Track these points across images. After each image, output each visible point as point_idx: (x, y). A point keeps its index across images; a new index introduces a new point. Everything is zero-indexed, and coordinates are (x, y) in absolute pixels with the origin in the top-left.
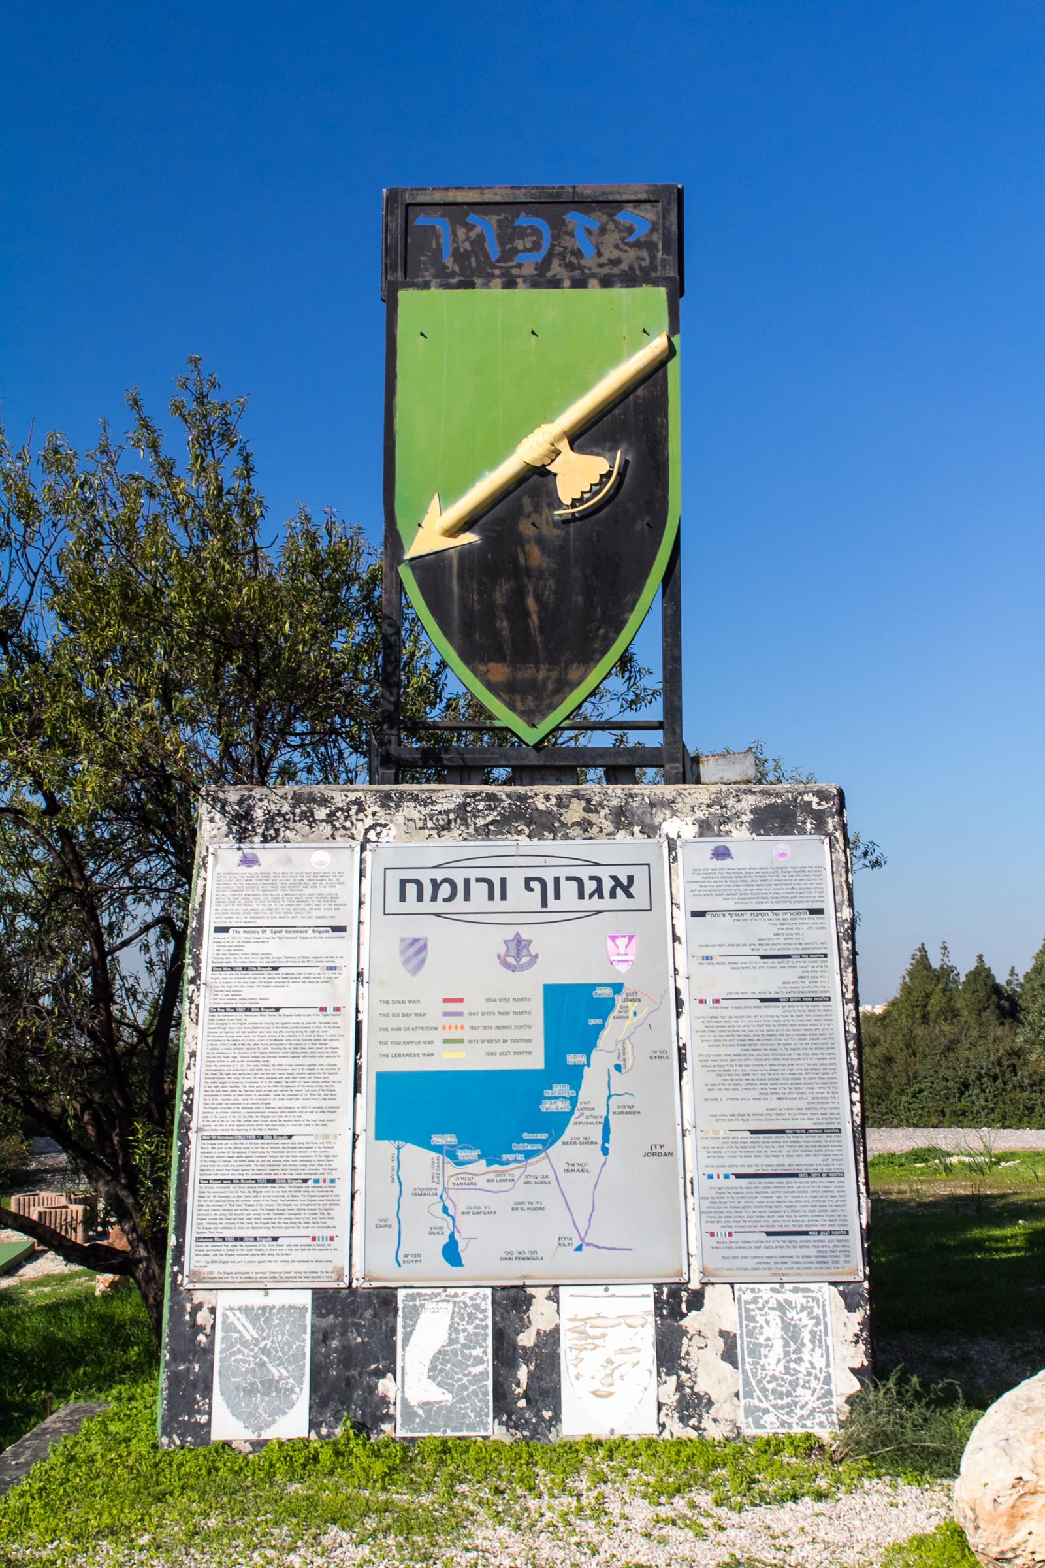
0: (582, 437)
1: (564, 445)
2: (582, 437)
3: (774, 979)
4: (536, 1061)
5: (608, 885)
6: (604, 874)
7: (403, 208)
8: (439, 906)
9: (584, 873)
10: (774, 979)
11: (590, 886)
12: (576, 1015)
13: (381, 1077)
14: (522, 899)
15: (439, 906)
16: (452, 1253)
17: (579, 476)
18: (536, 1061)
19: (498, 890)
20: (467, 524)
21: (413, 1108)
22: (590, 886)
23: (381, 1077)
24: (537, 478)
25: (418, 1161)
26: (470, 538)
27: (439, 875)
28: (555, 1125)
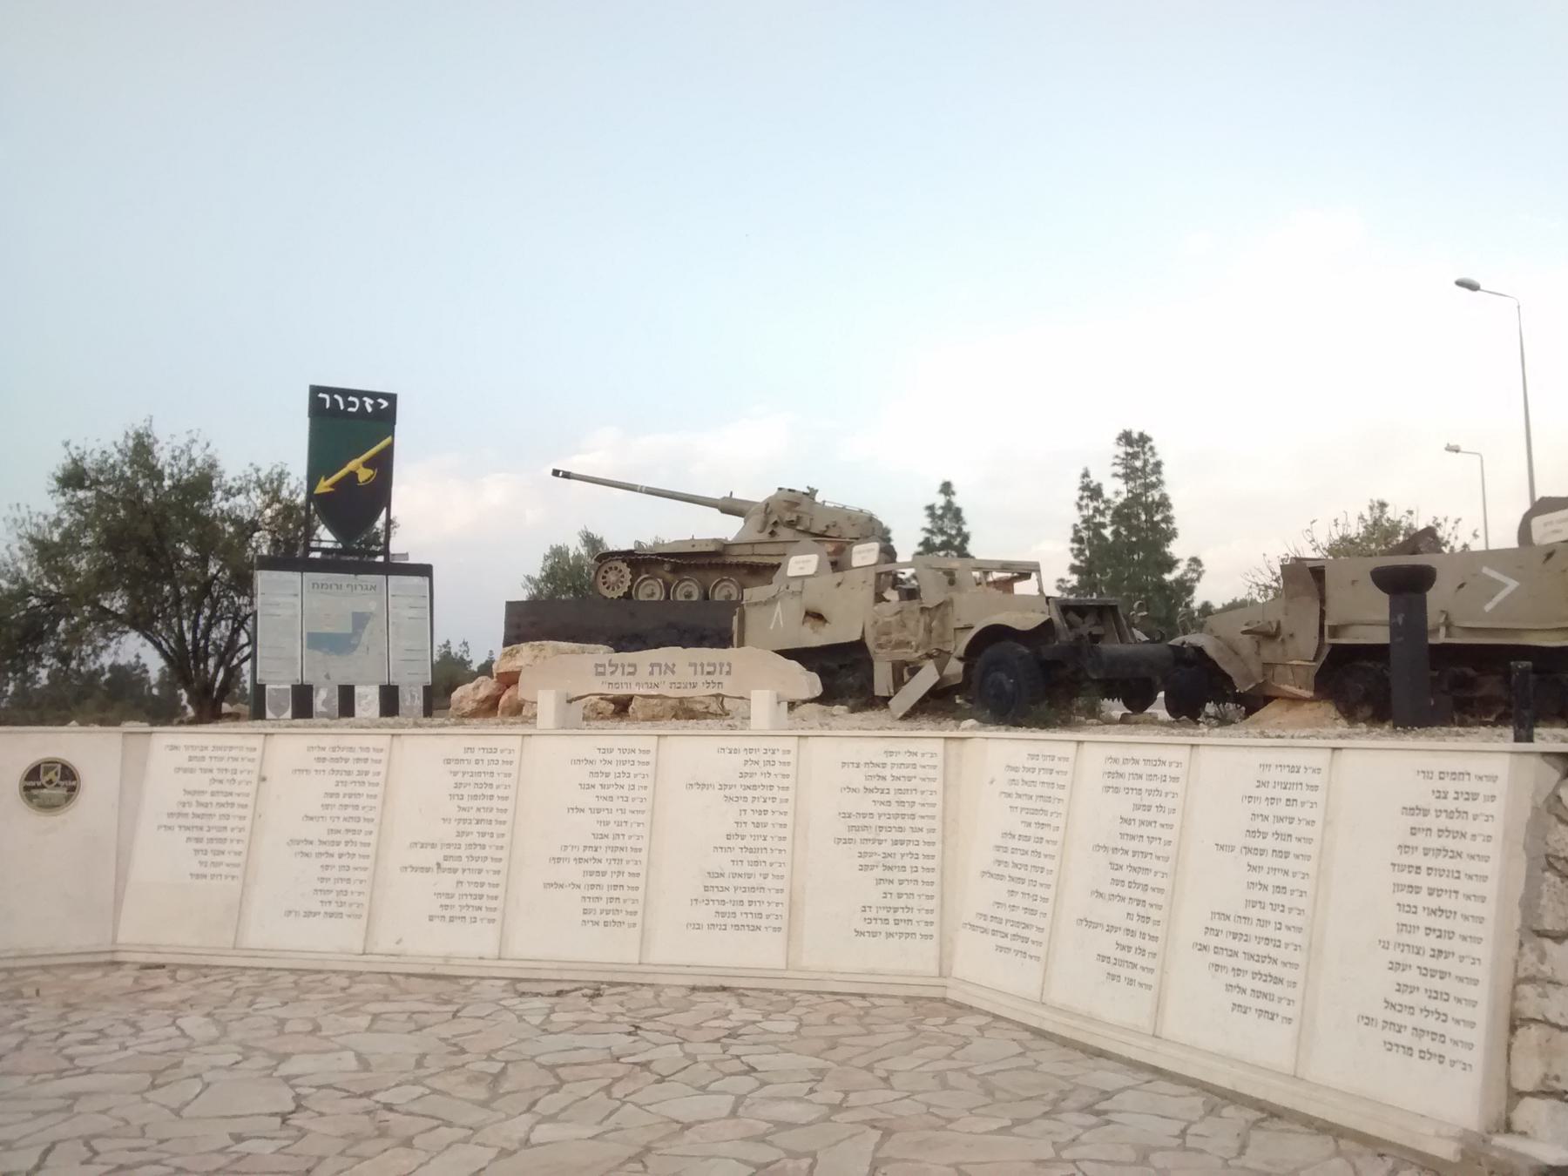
0: (367, 464)
2: (367, 464)
3: (412, 613)
4: (349, 630)
7: (315, 391)
10: (412, 613)
12: (360, 620)
13: (309, 634)
16: (328, 677)
17: (364, 475)
18: (349, 630)
20: (332, 486)
21: (317, 641)
23: (309, 634)
24: (353, 475)
25: (318, 654)
28: (354, 647)
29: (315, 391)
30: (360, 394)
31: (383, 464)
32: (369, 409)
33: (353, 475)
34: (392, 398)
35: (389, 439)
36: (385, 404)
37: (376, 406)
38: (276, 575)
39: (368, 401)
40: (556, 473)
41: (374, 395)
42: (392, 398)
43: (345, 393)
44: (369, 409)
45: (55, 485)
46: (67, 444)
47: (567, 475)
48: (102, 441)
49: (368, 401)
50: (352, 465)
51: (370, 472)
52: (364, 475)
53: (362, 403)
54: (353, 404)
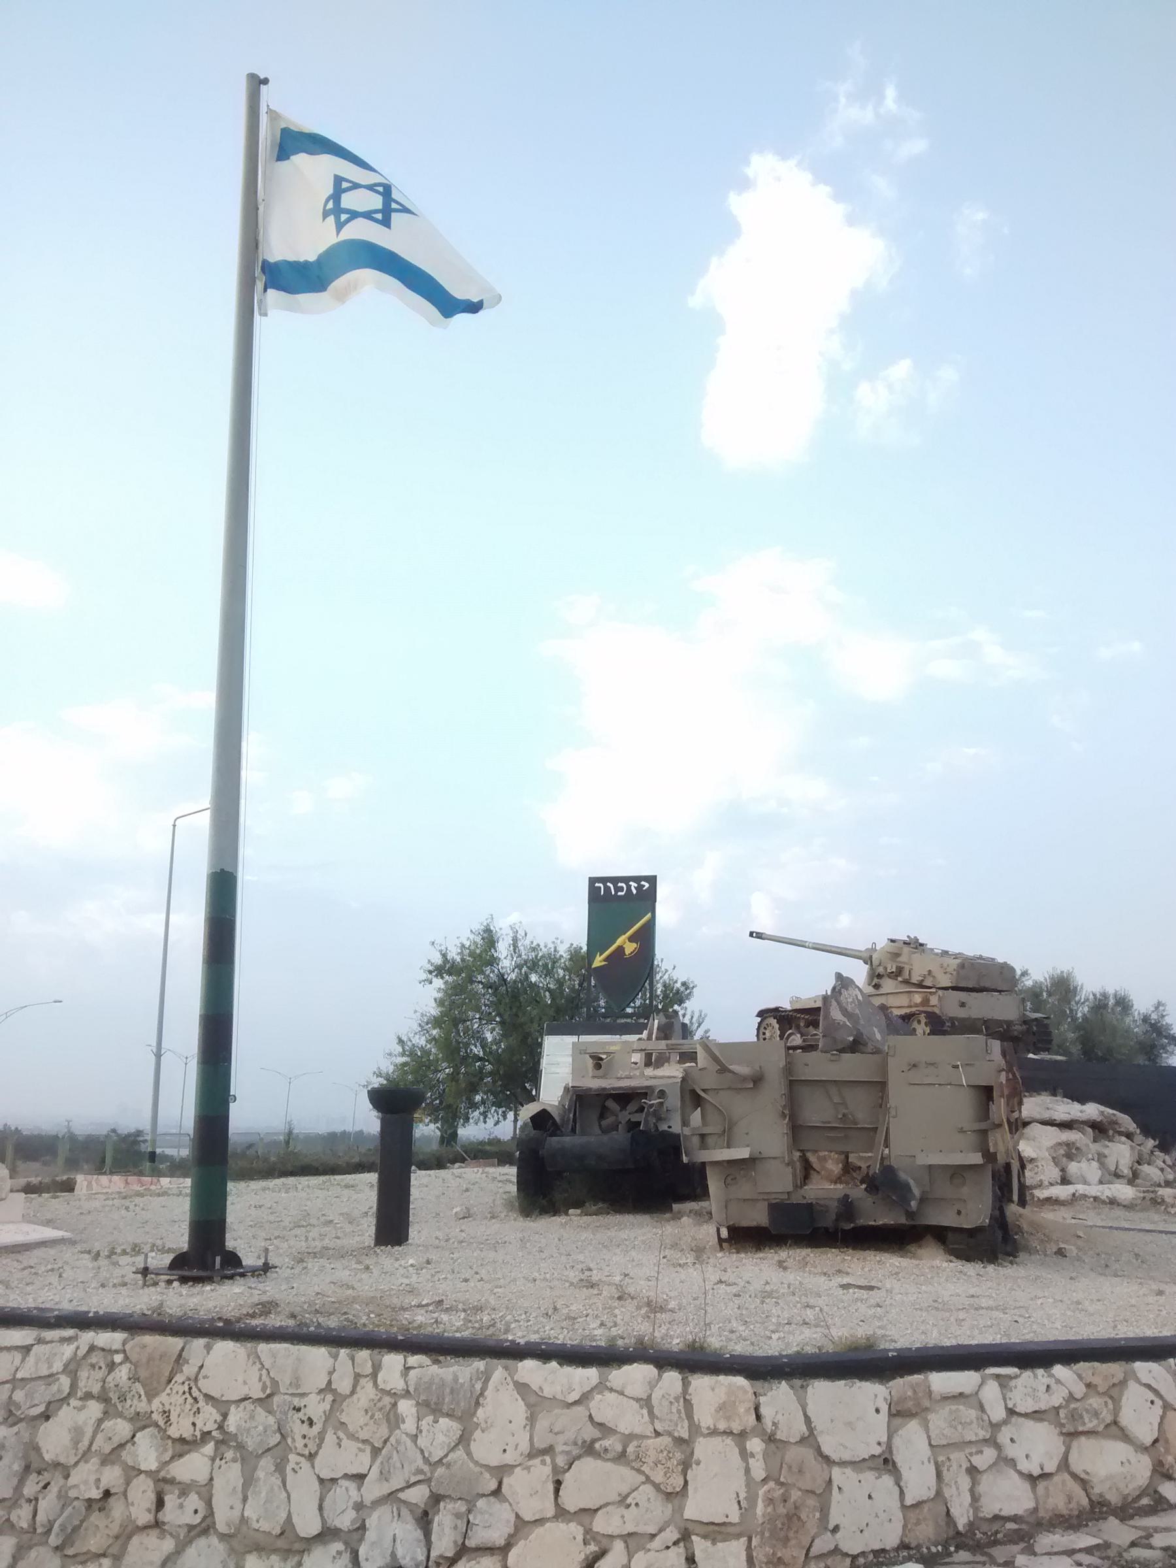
0: (631, 939)
2: (631, 939)
7: (592, 881)
17: (630, 948)
20: (605, 960)
24: (621, 949)
29: (592, 881)
30: (626, 880)
31: (646, 937)
32: (634, 892)
33: (621, 949)
34: (652, 880)
35: (649, 915)
36: (647, 885)
37: (639, 888)
39: (633, 884)
41: (637, 879)
42: (652, 880)
43: (615, 880)
44: (634, 892)
45: (424, 976)
47: (760, 936)
48: (456, 938)
49: (633, 884)
50: (619, 942)
51: (634, 945)
52: (630, 948)
53: (629, 887)
54: (621, 889)
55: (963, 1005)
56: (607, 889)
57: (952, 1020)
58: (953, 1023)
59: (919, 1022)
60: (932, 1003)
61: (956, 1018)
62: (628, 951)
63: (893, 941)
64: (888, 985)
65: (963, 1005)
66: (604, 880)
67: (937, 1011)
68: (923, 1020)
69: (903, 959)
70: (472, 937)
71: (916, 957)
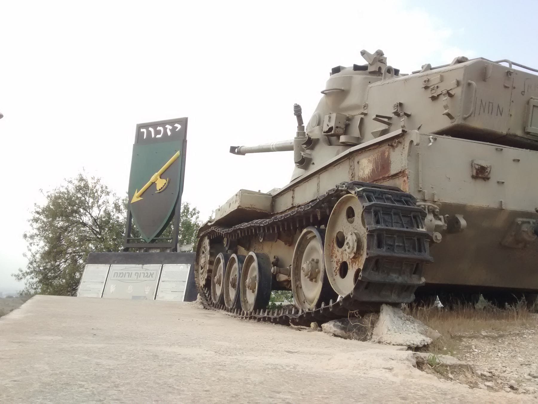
1: (159, 177)
5: (149, 274)
6: (149, 272)
8: (120, 278)
9: (145, 272)
11: (146, 275)
14: (134, 277)
15: (120, 278)
17: (161, 184)
19: (130, 275)
20: (141, 196)
22: (146, 275)
26: (140, 199)
27: (121, 272)
30: (163, 124)
32: (169, 133)
33: (153, 184)
34: (184, 122)
36: (179, 126)
37: (173, 130)
38: (103, 268)
40: (233, 150)
41: (172, 122)
42: (184, 122)
43: (155, 125)
44: (169, 133)
46: (41, 191)
49: (169, 127)
50: (152, 179)
53: (165, 129)
54: (158, 132)
55: (481, 174)
56: (149, 133)
57: (450, 212)
58: (453, 226)
59: (351, 214)
60: (394, 170)
61: (461, 209)
62: (158, 188)
63: (336, 70)
64: (324, 156)
65: (481, 174)
66: (146, 126)
67: (406, 186)
68: (358, 207)
69: (352, 100)
70: (66, 184)
71: (377, 85)
